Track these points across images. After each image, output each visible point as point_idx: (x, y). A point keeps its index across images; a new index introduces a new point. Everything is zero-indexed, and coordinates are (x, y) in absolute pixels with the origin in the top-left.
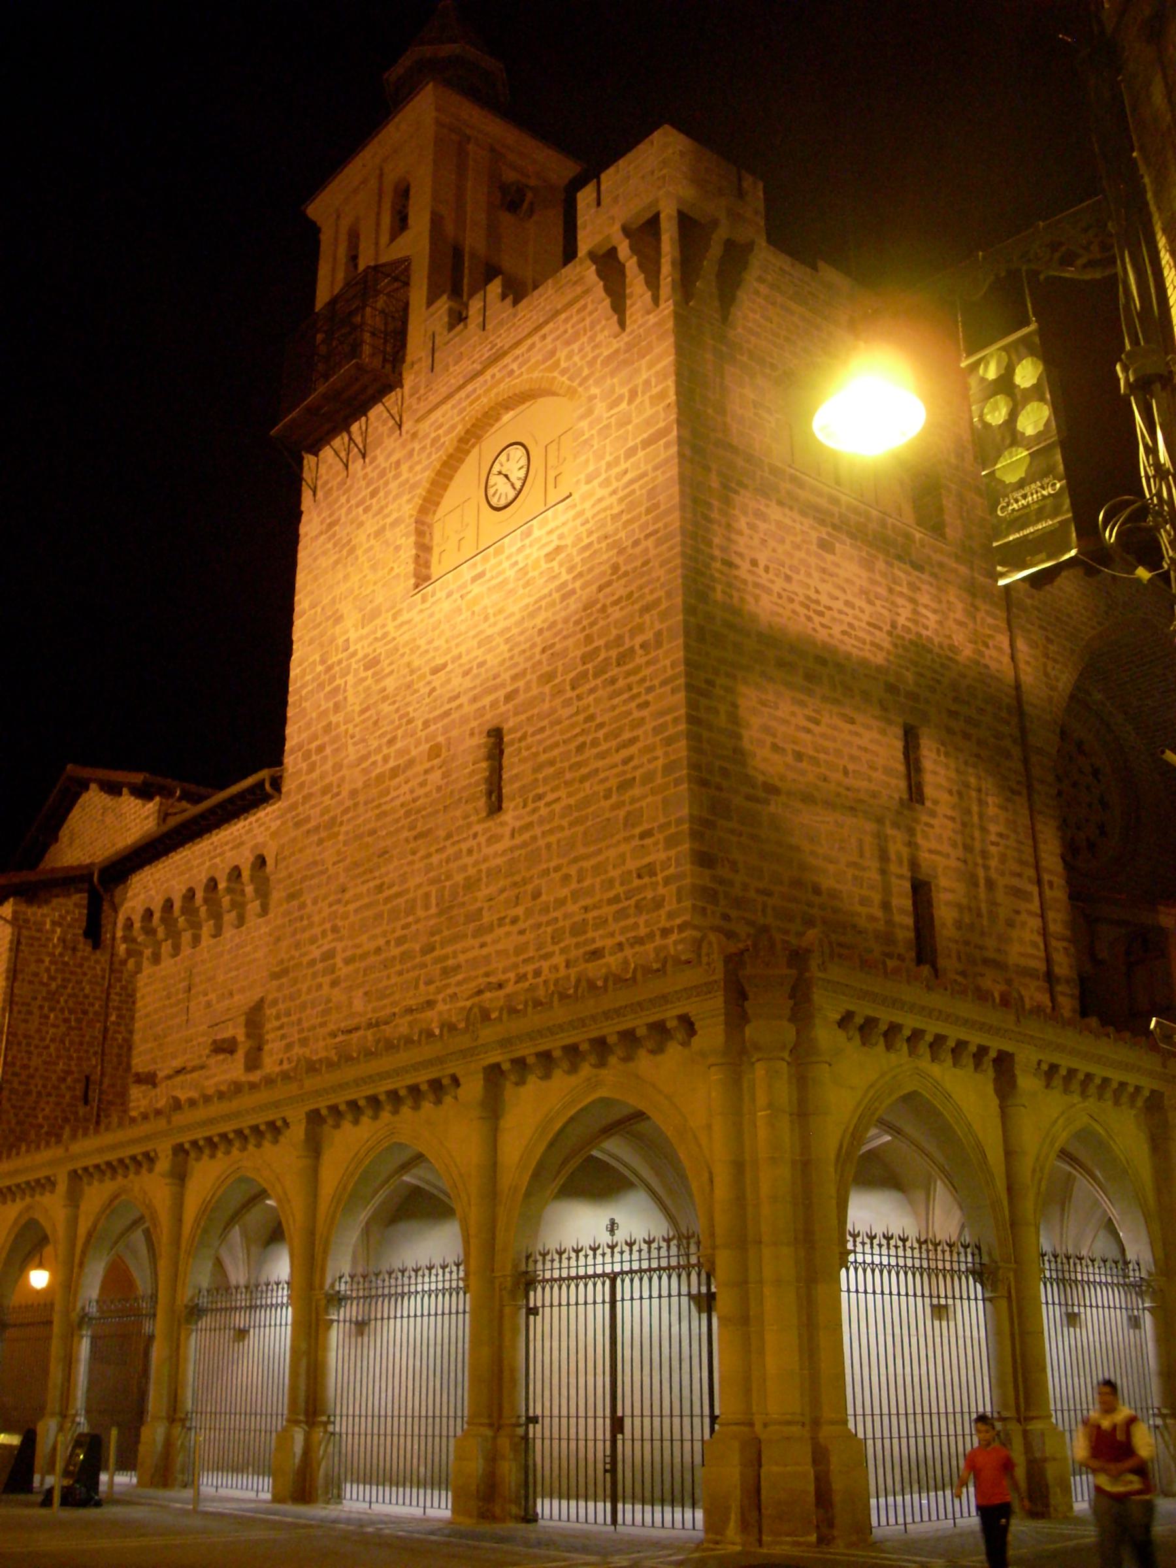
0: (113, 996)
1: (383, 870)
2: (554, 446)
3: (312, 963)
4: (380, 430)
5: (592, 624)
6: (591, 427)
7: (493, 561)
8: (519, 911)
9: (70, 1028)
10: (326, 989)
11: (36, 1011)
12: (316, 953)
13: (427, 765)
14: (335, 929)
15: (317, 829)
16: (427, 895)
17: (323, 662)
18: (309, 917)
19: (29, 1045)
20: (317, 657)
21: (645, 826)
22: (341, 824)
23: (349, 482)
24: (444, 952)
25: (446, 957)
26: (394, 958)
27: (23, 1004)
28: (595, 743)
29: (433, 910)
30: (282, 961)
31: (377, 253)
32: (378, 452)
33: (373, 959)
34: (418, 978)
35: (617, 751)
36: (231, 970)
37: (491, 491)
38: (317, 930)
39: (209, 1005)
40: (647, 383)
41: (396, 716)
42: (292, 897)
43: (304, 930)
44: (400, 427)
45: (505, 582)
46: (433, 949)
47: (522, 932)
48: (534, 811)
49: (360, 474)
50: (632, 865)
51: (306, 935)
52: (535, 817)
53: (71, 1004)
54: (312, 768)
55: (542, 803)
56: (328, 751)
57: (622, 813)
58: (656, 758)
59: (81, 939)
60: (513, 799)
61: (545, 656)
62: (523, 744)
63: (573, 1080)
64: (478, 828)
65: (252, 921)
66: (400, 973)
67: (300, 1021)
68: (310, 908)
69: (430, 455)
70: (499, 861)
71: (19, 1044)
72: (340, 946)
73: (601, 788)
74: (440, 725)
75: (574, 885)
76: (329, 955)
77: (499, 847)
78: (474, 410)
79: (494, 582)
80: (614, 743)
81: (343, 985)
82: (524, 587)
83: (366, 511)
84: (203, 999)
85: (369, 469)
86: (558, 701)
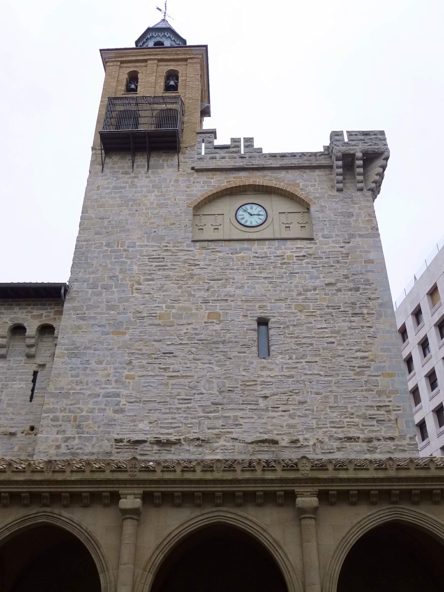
35: (356, 352)
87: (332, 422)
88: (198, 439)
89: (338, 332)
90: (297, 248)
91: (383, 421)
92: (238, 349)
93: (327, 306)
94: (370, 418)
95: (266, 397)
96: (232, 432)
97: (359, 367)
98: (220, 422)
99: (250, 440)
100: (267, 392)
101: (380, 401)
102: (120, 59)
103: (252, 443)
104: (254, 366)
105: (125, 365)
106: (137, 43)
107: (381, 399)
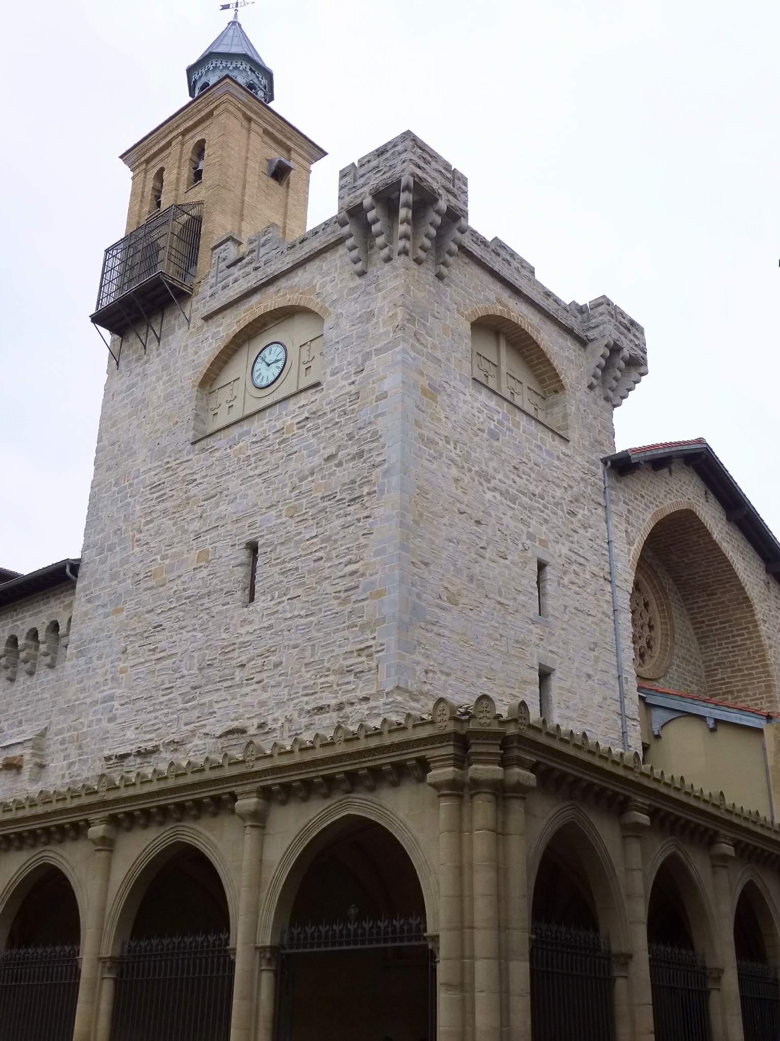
2: (306, 348)
3: (96, 703)
4: (173, 322)
5: (331, 474)
8: (264, 675)
12: (99, 696)
15: (104, 606)
17: (116, 484)
18: (94, 670)
22: (125, 602)
23: (145, 358)
24: (202, 701)
26: (161, 703)
28: (329, 559)
31: (177, 196)
32: (170, 337)
33: (142, 704)
34: (178, 719)
35: (346, 565)
36: (21, 706)
37: (256, 374)
42: (81, 653)
43: (89, 678)
44: (189, 321)
45: (265, 438)
47: (264, 689)
51: (92, 682)
52: (280, 608)
54: (103, 562)
55: (285, 598)
56: (118, 549)
57: (349, 607)
60: (263, 594)
61: (293, 494)
62: (273, 556)
63: (328, 802)
65: (42, 671)
66: (166, 715)
67: (80, 747)
68: (96, 663)
69: (211, 344)
74: (208, 537)
76: (111, 698)
78: (249, 318)
79: (254, 439)
81: (119, 721)
82: (280, 443)
83: (158, 379)
85: (161, 350)
86: (302, 526)
87: (305, 688)
88: (173, 742)
89: (328, 539)
90: (300, 408)
91: (362, 672)
92: (221, 601)
93: (322, 498)
94: (348, 671)
95: (243, 666)
96: (204, 726)
97: (346, 591)
98: (196, 713)
99: (218, 734)
100: (243, 658)
101: (362, 642)
102: (143, 159)
103: (220, 737)
104: (234, 621)
105: (120, 656)
106: (191, 94)
107: (365, 636)
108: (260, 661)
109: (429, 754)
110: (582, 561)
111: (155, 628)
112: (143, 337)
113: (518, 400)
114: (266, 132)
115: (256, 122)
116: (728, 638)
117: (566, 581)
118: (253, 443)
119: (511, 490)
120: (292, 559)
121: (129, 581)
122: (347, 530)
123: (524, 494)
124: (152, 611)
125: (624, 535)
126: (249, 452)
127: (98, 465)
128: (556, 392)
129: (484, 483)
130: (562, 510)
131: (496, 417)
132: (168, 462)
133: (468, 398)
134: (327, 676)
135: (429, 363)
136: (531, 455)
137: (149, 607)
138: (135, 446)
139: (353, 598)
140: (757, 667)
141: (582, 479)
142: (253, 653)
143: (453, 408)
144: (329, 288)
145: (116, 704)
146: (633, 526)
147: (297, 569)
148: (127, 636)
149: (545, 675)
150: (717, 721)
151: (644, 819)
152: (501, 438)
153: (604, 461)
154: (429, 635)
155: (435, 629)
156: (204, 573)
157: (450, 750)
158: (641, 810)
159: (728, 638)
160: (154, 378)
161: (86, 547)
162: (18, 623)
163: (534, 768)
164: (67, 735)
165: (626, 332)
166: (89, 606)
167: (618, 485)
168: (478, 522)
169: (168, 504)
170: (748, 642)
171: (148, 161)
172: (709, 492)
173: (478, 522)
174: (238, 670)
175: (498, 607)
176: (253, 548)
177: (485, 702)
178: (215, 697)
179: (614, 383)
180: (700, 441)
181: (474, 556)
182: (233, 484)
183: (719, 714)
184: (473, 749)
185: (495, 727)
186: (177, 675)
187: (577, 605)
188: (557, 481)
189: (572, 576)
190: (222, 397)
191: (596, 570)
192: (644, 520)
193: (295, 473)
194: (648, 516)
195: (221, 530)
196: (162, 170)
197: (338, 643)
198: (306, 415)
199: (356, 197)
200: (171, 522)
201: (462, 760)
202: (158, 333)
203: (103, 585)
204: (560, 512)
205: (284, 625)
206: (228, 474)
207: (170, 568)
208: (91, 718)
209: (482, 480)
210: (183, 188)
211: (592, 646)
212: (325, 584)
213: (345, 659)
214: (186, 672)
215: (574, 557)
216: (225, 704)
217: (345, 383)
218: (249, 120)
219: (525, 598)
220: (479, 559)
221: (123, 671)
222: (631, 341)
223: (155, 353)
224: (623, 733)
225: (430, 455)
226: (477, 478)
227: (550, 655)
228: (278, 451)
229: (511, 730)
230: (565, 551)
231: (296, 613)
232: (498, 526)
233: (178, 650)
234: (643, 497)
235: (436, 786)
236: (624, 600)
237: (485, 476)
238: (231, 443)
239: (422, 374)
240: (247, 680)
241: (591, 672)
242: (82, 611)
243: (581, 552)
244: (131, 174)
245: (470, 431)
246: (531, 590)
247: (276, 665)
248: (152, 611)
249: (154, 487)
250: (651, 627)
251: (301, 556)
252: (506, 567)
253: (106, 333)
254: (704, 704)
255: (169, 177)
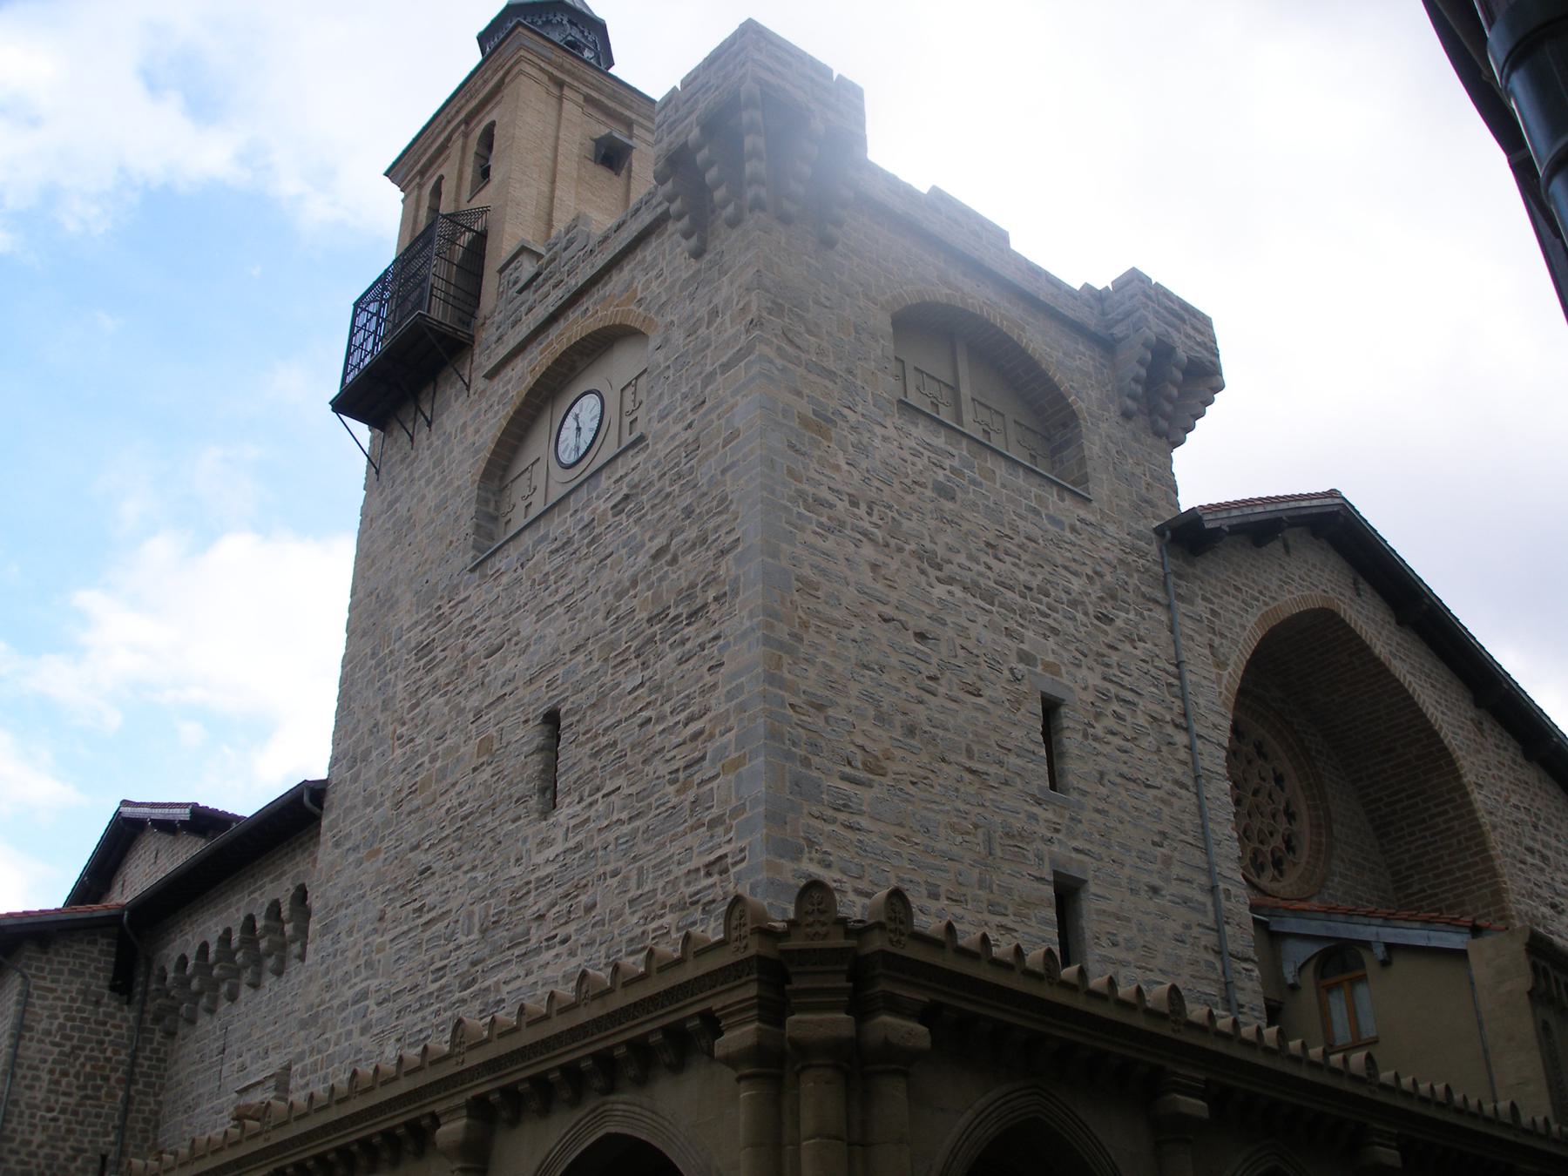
0: (140, 1060)
1: (426, 888)
5: (661, 579)
6: (667, 359)
7: (556, 521)
8: (571, 928)
9: (87, 1097)
10: (356, 1034)
11: (45, 1077)
12: (349, 994)
13: (476, 762)
14: (369, 964)
15: (355, 849)
16: (470, 915)
19: (33, 1116)
20: (369, 651)
21: (715, 811)
24: (487, 983)
25: (487, 989)
26: (431, 994)
27: (30, 1067)
28: (661, 718)
29: (475, 936)
30: (311, 1007)
33: (407, 998)
35: (686, 725)
38: (350, 967)
39: (243, 1068)
40: (728, 300)
41: (446, 710)
45: (569, 542)
46: (474, 981)
47: (572, 954)
48: (591, 804)
49: (425, 443)
50: (699, 861)
51: (339, 973)
52: (592, 812)
53: (88, 1068)
55: (600, 795)
56: (374, 754)
57: (690, 796)
58: (730, 730)
59: (107, 992)
63: (579, 1114)
64: (530, 831)
66: (437, 1013)
68: (346, 941)
69: (497, 412)
70: (550, 869)
71: (21, 1115)
72: (374, 983)
73: (664, 770)
75: (634, 893)
76: (364, 995)
77: (550, 853)
80: (682, 716)
83: (428, 483)
84: (238, 1061)
85: (434, 438)
87: (631, 940)
89: (658, 688)
91: (713, 901)
92: (510, 815)
93: (649, 620)
94: (692, 904)
95: (541, 917)
97: (687, 767)
105: (377, 925)
107: (716, 840)
108: (565, 905)
109: (716, 1004)
110: (1129, 696)
111: (422, 873)
112: (409, 426)
113: (997, 442)
114: (588, 100)
115: (571, 87)
116: (1424, 820)
117: (1099, 729)
118: (552, 552)
119: (982, 581)
120: (606, 730)
121: (388, 804)
122: (685, 666)
123: (1010, 588)
124: (417, 846)
125: (1207, 652)
126: (547, 568)
127: (351, 629)
128: (1065, 425)
129: (929, 570)
130: (1086, 614)
131: (947, 463)
132: (439, 607)
133: (891, 432)
134: (662, 916)
135: (813, 377)
136: (1020, 523)
137: (414, 841)
138: (398, 592)
139: (697, 778)
140: (1476, 864)
141: (1121, 561)
142: (555, 893)
143: (862, 449)
144: (654, 285)
145: (371, 1003)
146: (1222, 636)
147: (615, 743)
148: (386, 893)
149: (1067, 894)
150: (1390, 947)
151: (1195, 1106)
152: (959, 495)
153: (1159, 531)
154: (828, 828)
155: (842, 817)
156: (486, 774)
157: (752, 990)
158: (1189, 1091)
159: (1424, 820)
160: (423, 482)
161: (335, 761)
162: (256, 895)
163: (927, 1015)
164: (308, 1061)
165: (1178, 323)
166: (338, 852)
167: (1189, 570)
168: (921, 636)
169: (439, 672)
170: (1456, 823)
171: (422, 173)
172: (1361, 580)
173: (921, 636)
174: (535, 925)
175: (967, 777)
176: (552, 719)
177: (816, 895)
178: (503, 975)
179: (1168, 408)
180: (1333, 493)
181: (915, 692)
182: (527, 626)
183: (1392, 935)
184: (797, 984)
185: (839, 941)
186: (451, 946)
187: (1125, 769)
188: (1074, 566)
189: (1110, 722)
190: (519, 489)
191: (1158, 710)
192: (1243, 627)
193: (610, 587)
194: (1251, 620)
195: (509, 701)
196: (441, 178)
197: (676, 858)
198: (625, 491)
199: (677, 136)
200: (442, 700)
201: (773, 1010)
202: (428, 414)
203: (355, 815)
204: (1080, 616)
205: (597, 842)
206: (518, 609)
207: (443, 771)
208: (339, 1031)
209: (925, 566)
210: (466, 195)
211: (1157, 839)
212: (657, 761)
213: (688, 884)
214: (463, 939)
215: (1113, 689)
216: (517, 984)
217: (679, 427)
218: (561, 85)
219: (1019, 762)
220: (927, 697)
221: (380, 949)
222: (1188, 336)
223: (425, 443)
224: (1226, 984)
225: (820, 525)
226: (915, 562)
227: (1074, 855)
228: (586, 557)
229: (877, 942)
230: (1094, 680)
231: (615, 818)
232: (959, 641)
233: (453, 905)
234: (1238, 589)
235: (730, 1061)
236: (1214, 759)
237: (929, 559)
238: (523, 559)
239: (799, 394)
240: (547, 940)
241: (1158, 883)
242: (328, 866)
243: (1127, 681)
244: (402, 195)
245: (897, 486)
246: (1031, 747)
247: (590, 908)
248: (417, 846)
249: (423, 649)
250: (1291, 816)
251: (620, 722)
252: (982, 709)
253: (363, 431)
254: (1366, 921)
255: (448, 188)
